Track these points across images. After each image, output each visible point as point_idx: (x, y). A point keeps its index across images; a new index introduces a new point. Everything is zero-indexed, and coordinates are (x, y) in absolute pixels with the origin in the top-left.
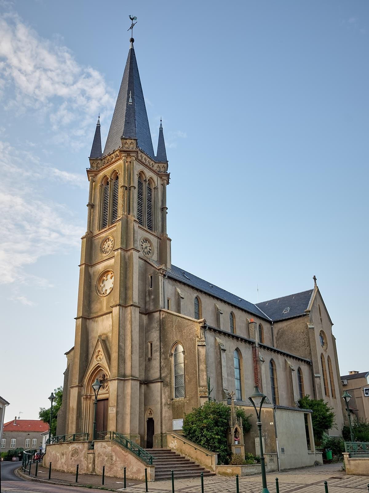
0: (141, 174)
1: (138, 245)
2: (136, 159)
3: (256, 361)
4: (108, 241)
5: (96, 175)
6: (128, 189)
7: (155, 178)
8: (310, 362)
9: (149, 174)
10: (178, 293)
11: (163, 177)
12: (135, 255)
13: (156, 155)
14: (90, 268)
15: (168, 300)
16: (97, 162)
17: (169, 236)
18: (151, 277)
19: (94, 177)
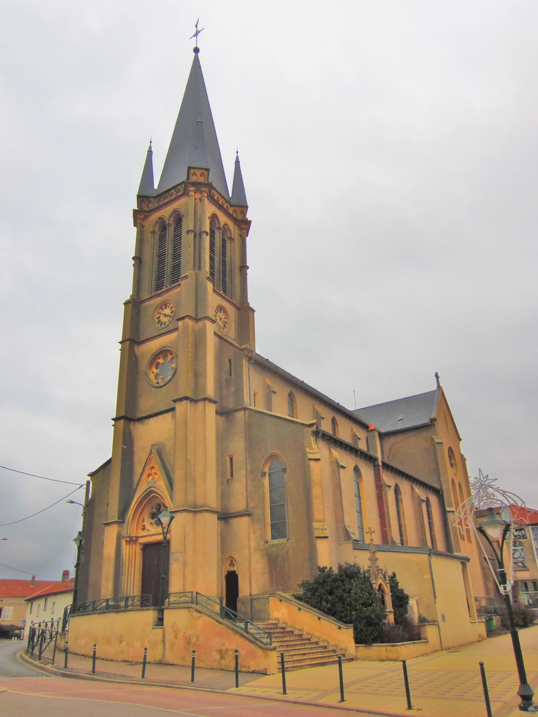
0: (214, 217)
1: (211, 313)
2: (208, 196)
3: (380, 486)
4: (166, 308)
5: (146, 217)
6: (198, 235)
7: (231, 225)
8: (439, 491)
9: (223, 219)
10: (269, 385)
11: (241, 226)
12: (210, 328)
13: (230, 196)
14: (136, 347)
15: (254, 395)
16: (148, 201)
17: (251, 305)
18: (230, 361)
19: (143, 220)
